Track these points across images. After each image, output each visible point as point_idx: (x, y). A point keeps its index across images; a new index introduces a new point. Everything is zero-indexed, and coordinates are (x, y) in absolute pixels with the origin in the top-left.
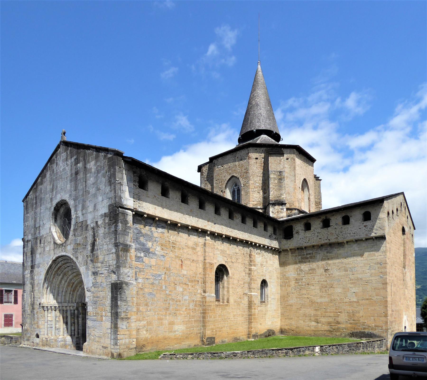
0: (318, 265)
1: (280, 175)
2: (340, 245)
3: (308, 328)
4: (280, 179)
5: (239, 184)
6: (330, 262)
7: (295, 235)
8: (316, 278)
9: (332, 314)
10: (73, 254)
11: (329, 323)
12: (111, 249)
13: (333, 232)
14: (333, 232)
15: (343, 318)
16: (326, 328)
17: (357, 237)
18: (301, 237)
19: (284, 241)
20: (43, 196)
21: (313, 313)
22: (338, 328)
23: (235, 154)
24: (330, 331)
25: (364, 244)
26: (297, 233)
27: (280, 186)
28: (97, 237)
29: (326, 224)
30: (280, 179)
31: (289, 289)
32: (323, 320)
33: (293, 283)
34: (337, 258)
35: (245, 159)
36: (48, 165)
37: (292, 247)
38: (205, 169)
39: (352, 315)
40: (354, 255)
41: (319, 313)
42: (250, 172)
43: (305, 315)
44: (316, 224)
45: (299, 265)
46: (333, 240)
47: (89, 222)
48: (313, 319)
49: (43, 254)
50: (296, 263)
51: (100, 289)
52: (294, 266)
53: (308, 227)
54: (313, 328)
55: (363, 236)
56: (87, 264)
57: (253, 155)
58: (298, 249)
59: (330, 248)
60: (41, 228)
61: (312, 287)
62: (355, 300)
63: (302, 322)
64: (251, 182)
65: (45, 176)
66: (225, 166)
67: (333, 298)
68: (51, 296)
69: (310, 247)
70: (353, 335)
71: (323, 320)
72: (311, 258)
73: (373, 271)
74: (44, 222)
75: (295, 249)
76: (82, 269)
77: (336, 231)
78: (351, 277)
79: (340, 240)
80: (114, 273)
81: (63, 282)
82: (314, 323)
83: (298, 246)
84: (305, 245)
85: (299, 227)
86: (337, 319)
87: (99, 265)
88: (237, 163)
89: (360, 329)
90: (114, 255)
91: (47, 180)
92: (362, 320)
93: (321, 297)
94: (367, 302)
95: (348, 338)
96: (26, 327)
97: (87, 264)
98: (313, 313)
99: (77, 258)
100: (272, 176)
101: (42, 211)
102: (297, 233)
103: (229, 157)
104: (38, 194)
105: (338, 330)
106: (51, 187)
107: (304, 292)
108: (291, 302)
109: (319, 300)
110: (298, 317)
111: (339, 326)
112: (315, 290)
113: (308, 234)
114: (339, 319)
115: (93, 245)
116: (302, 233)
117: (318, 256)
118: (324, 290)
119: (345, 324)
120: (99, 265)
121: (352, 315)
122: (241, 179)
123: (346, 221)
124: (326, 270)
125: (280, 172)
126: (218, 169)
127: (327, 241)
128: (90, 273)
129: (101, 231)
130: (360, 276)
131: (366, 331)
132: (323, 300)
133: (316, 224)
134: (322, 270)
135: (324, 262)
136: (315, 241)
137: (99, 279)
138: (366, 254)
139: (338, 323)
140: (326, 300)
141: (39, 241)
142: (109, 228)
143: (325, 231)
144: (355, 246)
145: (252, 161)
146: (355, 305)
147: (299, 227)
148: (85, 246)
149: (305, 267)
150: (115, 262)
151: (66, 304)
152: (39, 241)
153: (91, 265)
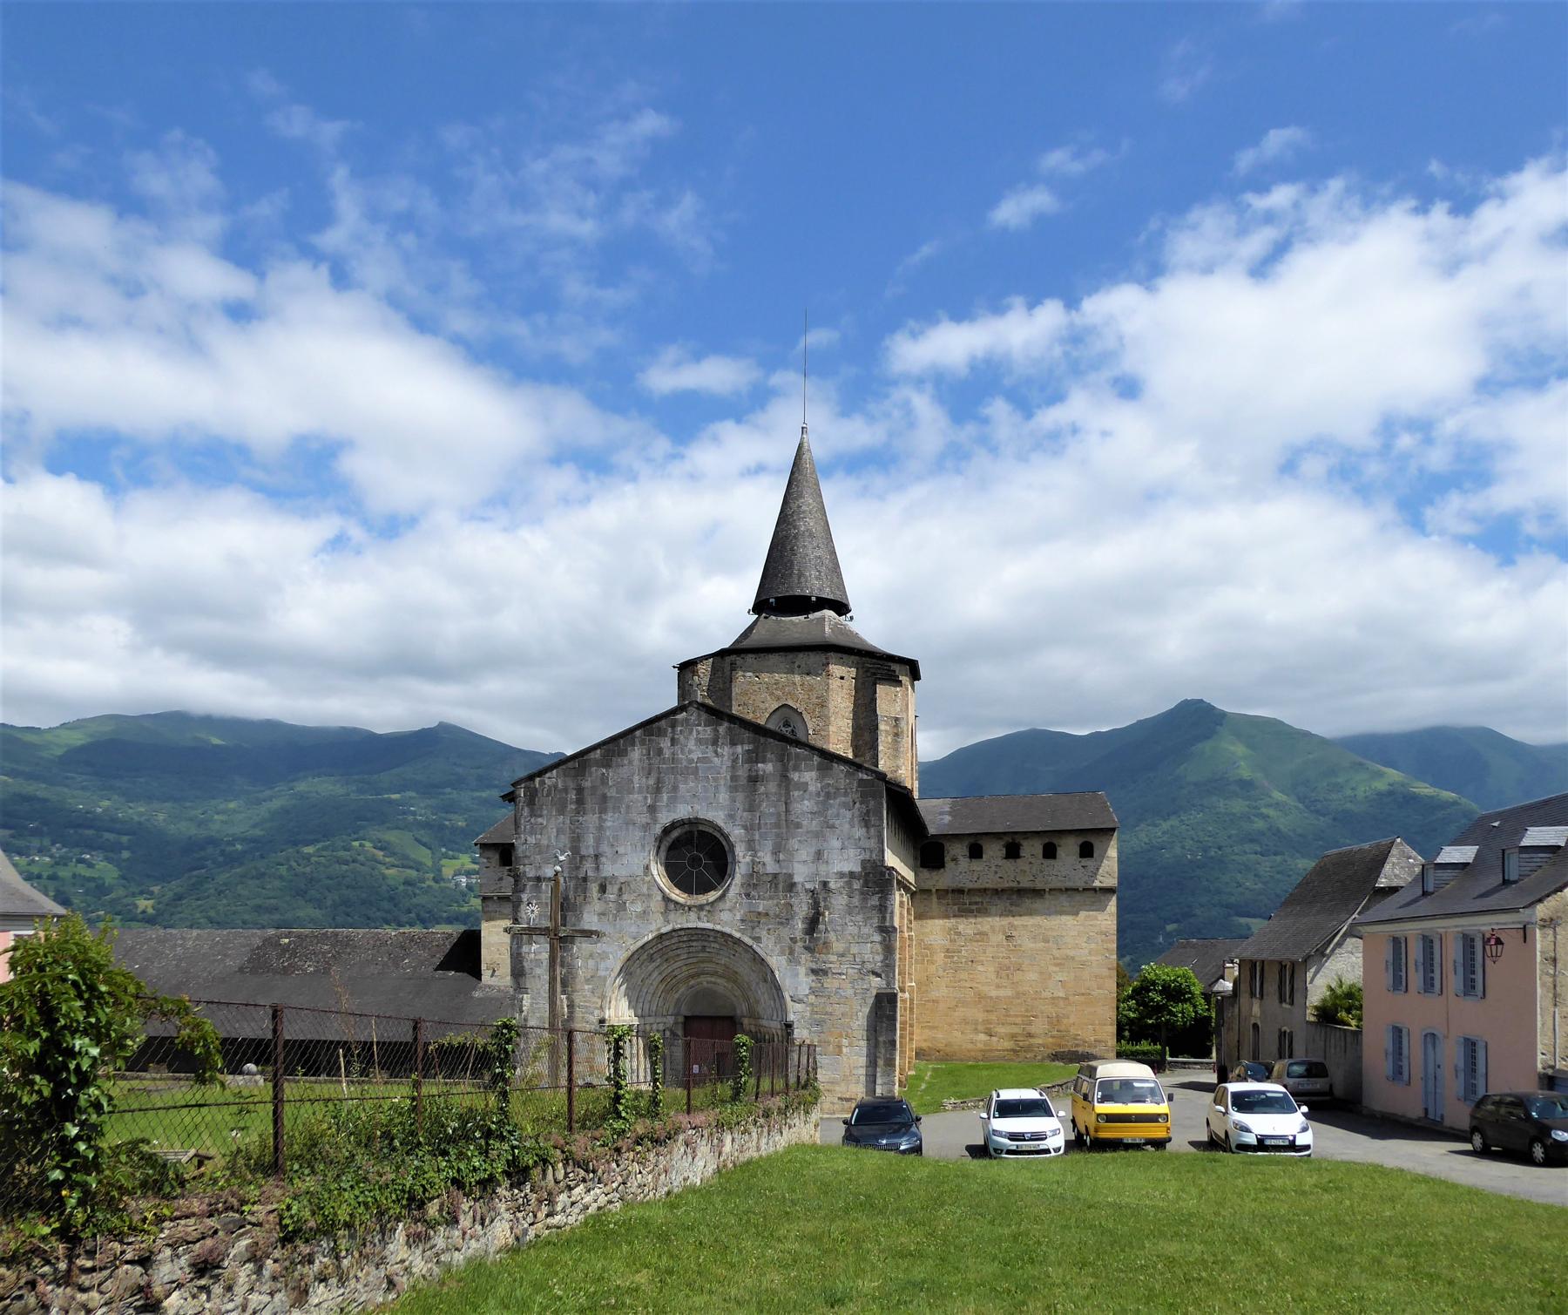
0: (993, 924)
1: (896, 726)
2: (1037, 893)
3: (970, 1046)
4: (896, 735)
5: (799, 725)
6: (1017, 921)
7: (949, 865)
8: (989, 950)
9: (1019, 1020)
10: (742, 931)
11: (1013, 1036)
12: (869, 936)
13: (1026, 868)
14: (1026, 868)
15: (1039, 1027)
16: (1008, 1044)
17: (1069, 884)
18: (959, 870)
19: (925, 873)
20: (612, 793)
21: (981, 1016)
22: (1031, 1046)
23: (790, 656)
24: (1014, 1050)
25: (1078, 897)
26: (954, 860)
27: (897, 750)
28: (827, 908)
29: (1013, 852)
30: (896, 735)
31: (932, 969)
32: (1001, 1030)
33: (940, 957)
34: (1030, 913)
35: (817, 675)
36: (638, 733)
37: (941, 886)
38: (704, 669)
39: (1055, 1021)
40: (1062, 913)
41: (993, 1017)
42: (831, 705)
43: (965, 1021)
44: (994, 851)
45: (953, 921)
46: (1025, 884)
47: (797, 879)
48: (980, 1028)
49: (615, 916)
50: (948, 917)
51: (835, 999)
52: (940, 922)
53: (976, 852)
54: (980, 1046)
55: (1080, 884)
56: (792, 952)
57: (837, 670)
58: (953, 891)
59: (1019, 897)
60: (603, 860)
61: (980, 968)
62: (1062, 994)
63: (958, 1034)
64: (832, 728)
65: (623, 753)
66: (766, 677)
67: (1020, 989)
68: (624, 1003)
69: (979, 890)
70: (1056, 1057)
71: (1001, 1030)
72: (979, 911)
73: (1093, 946)
74: (621, 850)
75: (946, 891)
76: (777, 961)
77: (1030, 868)
78: (1056, 952)
79: (1039, 886)
80: (878, 975)
81: (655, 974)
82: (982, 1037)
83: (954, 886)
84: (971, 886)
85: (958, 850)
86: (1028, 1028)
87: (833, 958)
88: (797, 678)
89: (1069, 1046)
90: (878, 947)
91: (630, 762)
92: (1073, 1031)
93: (998, 987)
94: (1082, 998)
95: (1047, 1062)
96: (530, 1071)
97: (792, 952)
98: (981, 1016)
99: (758, 939)
100: (882, 727)
101: (609, 824)
102: (954, 860)
103: (774, 659)
104: (587, 784)
105: (1029, 1049)
106: (651, 782)
107: (964, 975)
108: (934, 995)
109: (994, 993)
110: (950, 1025)
111: (1033, 1041)
112: (986, 973)
113: (977, 865)
114: (1033, 1029)
115: (813, 923)
116: (964, 862)
117: (993, 909)
118: (1004, 974)
119: (1043, 1037)
120: (833, 958)
121: (1055, 1021)
122: (806, 717)
123: (1050, 852)
124: (1009, 937)
125: (897, 719)
126: (744, 681)
127: (1015, 885)
128: (802, 970)
129: (839, 901)
130: (1071, 953)
131: (1080, 1049)
132: (1001, 993)
133: (994, 851)
134: (1001, 937)
135: (1006, 921)
136: (990, 881)
137: (830, 983)
138: (1083, 914)
139: (1030, 1035)
140: (1009, 993)
141: (594, 888)
142: (865, 900)
143: (1009, 864)
144: (1063, 898)
145: (835, 683)
146: (1062, 1003)
147: (958, 850)
148: (786, 920)
149: (967, 926)
150: (879, 958)
151: (651, 1020)
152: (594, 888)
153: (805, 957)
